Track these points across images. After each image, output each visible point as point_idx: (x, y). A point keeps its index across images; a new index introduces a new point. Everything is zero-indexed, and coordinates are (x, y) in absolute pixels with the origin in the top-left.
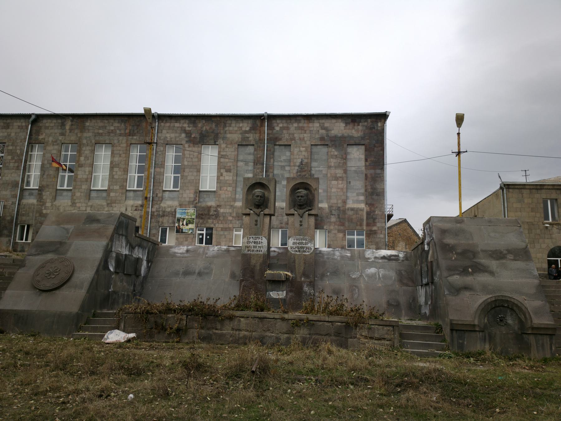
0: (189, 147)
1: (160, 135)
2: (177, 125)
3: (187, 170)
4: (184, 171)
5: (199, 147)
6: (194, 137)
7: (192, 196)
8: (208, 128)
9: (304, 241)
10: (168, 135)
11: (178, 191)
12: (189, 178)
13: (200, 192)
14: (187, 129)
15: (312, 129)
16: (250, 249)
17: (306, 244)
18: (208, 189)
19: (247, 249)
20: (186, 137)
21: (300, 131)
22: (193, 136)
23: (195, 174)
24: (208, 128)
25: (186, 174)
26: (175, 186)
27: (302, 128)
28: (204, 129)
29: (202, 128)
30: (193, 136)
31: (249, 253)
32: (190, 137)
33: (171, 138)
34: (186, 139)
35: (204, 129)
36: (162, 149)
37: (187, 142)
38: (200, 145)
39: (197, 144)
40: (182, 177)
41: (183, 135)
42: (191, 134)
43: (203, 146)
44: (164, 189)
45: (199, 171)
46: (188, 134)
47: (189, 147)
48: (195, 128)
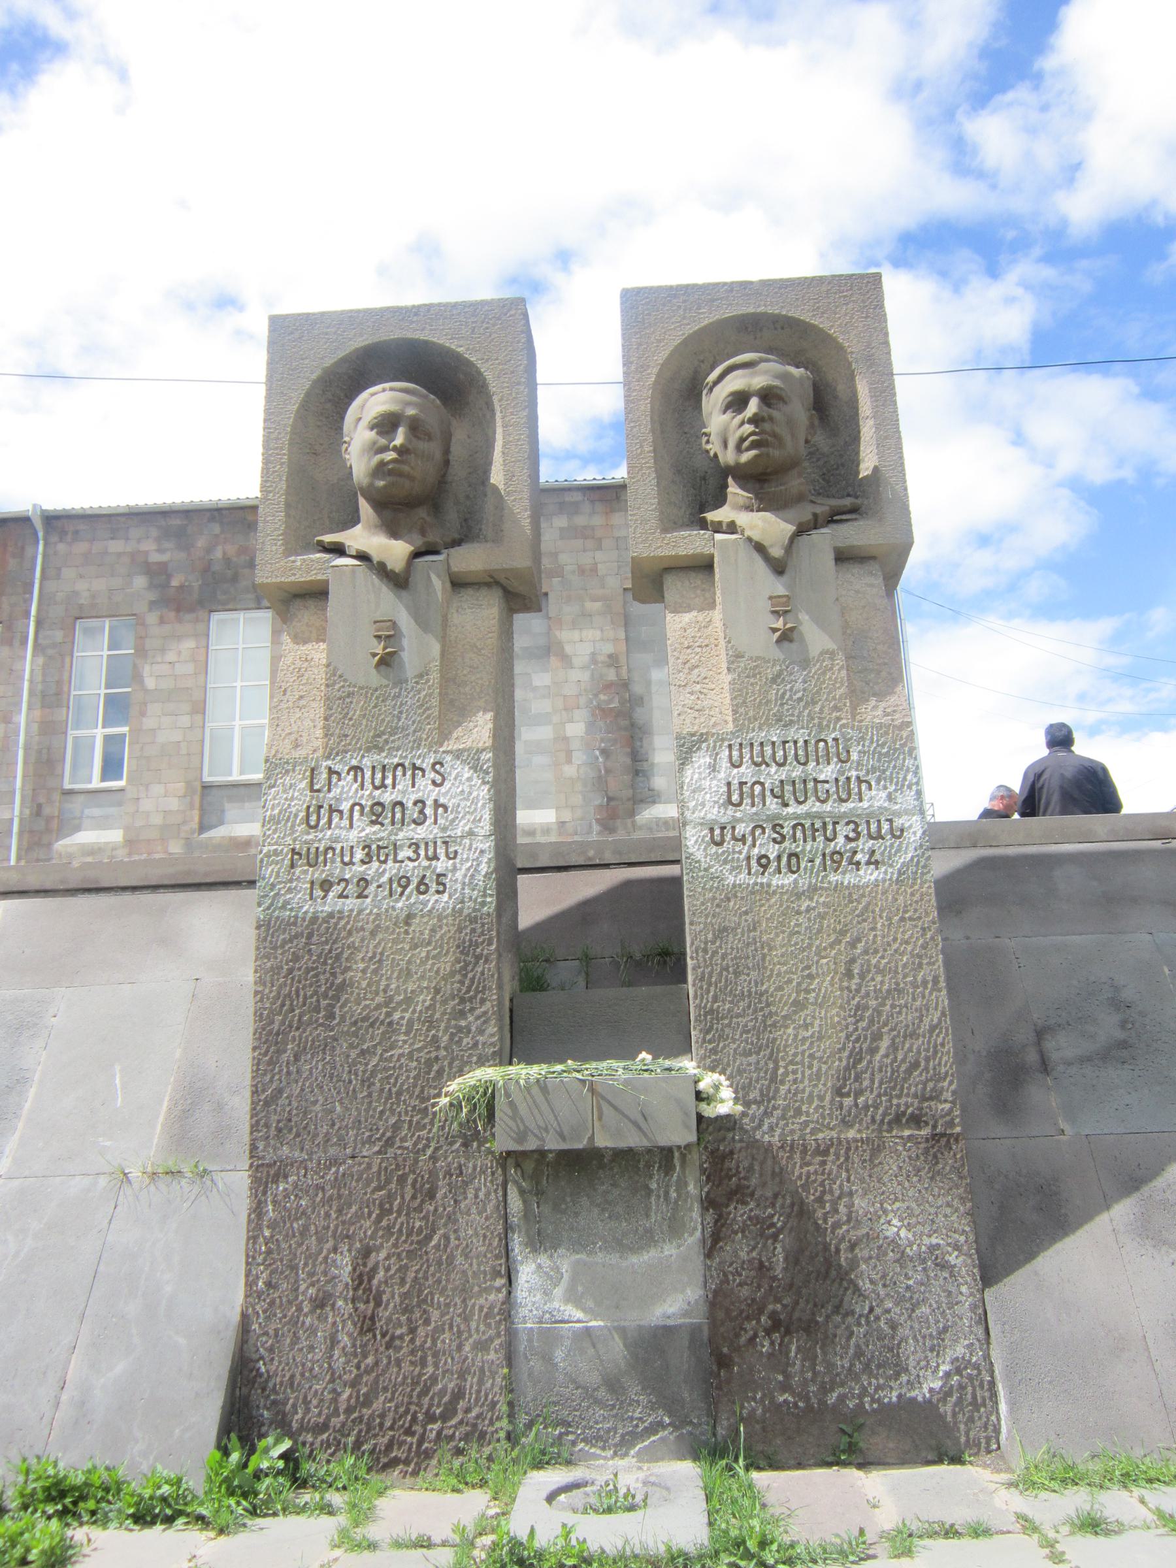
0: (162, 621)
1: (52, 586)
2: (116, 546)
3: (154, 709)
4: (143, 714)
5: (197, 620)
6: (181, 587)
7: (174, 804)
8: (231, 550)
9: (828, 772)
10: (81, 586)
11: (122, 790)
12: (162, 738)
13: (206, 787)
14: (155, 558)
15: (622, 533)
16: (334, 869)
17: (845, 790)
18: (236, 777)
19: (306, 874)
20: (151, 586)
21: (579, 543)
22: (175, 583)
23: (185, 720)
24: (231, 550)
25: (149, 723)
26: (111, 767)
27: (584, 533)
28: (218, 554)
29: (209, 550)
30: (175, 583)
31: (331, 903)
32: (165, 586)
33: (93, 597)
34: (152, 596)
35: (218, 554)
36: (59, 635)
37: (153, 605)
38: (202, 614)
39: (192, 610)
40: (136, 732)
41: (140, 582)
42: (169, 577)
43: (216, 617)
44: (67, 786)
45: (200, 708)
46: (158, 574)
47: (162, 621)
48: (182, 555)
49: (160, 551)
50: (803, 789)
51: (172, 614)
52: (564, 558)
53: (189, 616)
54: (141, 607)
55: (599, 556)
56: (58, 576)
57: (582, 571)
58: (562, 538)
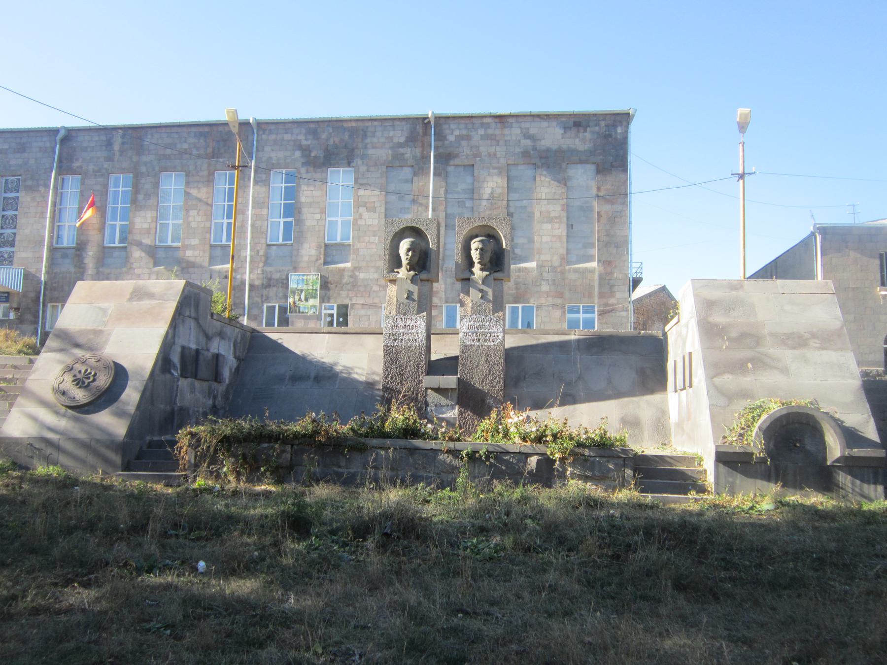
0: (307, 172)
2: (287, 137)
6: (315, 157)
8: (337, 140)
10: (273, 155)
13: (326, 245)
14: (304, 143)
15: (508, 138)
20: (303, 156)
22: (313, 155)
23: (318, 216)
24: (337, 140)
28: (331, 142)
29: (327, 140)
30: (313, 155)
33: (278, 159)
34: (302, 160)
36: (264, 176)
37: (304, 164)
38: (324, 169)
39: (320, 167)
41: (298, 154)
42: (310, 152)
46: (306, 151)
47: (307, 172)
49: (306, 140)
50: (481, 327)
51: (311, 169)
52: (482, 149)
53: (319, 170)
54: (299, 165)
55: (498, 148)
56: (263, 150)
57: (489, 155)
58: (482, 139)
